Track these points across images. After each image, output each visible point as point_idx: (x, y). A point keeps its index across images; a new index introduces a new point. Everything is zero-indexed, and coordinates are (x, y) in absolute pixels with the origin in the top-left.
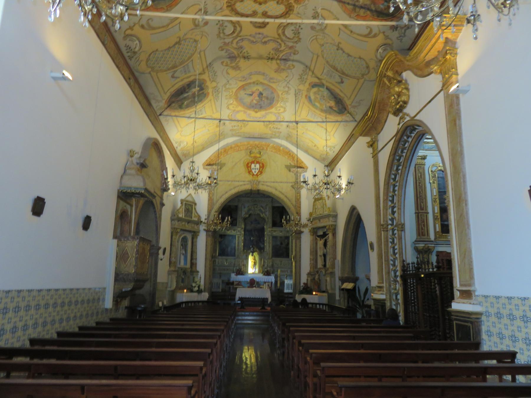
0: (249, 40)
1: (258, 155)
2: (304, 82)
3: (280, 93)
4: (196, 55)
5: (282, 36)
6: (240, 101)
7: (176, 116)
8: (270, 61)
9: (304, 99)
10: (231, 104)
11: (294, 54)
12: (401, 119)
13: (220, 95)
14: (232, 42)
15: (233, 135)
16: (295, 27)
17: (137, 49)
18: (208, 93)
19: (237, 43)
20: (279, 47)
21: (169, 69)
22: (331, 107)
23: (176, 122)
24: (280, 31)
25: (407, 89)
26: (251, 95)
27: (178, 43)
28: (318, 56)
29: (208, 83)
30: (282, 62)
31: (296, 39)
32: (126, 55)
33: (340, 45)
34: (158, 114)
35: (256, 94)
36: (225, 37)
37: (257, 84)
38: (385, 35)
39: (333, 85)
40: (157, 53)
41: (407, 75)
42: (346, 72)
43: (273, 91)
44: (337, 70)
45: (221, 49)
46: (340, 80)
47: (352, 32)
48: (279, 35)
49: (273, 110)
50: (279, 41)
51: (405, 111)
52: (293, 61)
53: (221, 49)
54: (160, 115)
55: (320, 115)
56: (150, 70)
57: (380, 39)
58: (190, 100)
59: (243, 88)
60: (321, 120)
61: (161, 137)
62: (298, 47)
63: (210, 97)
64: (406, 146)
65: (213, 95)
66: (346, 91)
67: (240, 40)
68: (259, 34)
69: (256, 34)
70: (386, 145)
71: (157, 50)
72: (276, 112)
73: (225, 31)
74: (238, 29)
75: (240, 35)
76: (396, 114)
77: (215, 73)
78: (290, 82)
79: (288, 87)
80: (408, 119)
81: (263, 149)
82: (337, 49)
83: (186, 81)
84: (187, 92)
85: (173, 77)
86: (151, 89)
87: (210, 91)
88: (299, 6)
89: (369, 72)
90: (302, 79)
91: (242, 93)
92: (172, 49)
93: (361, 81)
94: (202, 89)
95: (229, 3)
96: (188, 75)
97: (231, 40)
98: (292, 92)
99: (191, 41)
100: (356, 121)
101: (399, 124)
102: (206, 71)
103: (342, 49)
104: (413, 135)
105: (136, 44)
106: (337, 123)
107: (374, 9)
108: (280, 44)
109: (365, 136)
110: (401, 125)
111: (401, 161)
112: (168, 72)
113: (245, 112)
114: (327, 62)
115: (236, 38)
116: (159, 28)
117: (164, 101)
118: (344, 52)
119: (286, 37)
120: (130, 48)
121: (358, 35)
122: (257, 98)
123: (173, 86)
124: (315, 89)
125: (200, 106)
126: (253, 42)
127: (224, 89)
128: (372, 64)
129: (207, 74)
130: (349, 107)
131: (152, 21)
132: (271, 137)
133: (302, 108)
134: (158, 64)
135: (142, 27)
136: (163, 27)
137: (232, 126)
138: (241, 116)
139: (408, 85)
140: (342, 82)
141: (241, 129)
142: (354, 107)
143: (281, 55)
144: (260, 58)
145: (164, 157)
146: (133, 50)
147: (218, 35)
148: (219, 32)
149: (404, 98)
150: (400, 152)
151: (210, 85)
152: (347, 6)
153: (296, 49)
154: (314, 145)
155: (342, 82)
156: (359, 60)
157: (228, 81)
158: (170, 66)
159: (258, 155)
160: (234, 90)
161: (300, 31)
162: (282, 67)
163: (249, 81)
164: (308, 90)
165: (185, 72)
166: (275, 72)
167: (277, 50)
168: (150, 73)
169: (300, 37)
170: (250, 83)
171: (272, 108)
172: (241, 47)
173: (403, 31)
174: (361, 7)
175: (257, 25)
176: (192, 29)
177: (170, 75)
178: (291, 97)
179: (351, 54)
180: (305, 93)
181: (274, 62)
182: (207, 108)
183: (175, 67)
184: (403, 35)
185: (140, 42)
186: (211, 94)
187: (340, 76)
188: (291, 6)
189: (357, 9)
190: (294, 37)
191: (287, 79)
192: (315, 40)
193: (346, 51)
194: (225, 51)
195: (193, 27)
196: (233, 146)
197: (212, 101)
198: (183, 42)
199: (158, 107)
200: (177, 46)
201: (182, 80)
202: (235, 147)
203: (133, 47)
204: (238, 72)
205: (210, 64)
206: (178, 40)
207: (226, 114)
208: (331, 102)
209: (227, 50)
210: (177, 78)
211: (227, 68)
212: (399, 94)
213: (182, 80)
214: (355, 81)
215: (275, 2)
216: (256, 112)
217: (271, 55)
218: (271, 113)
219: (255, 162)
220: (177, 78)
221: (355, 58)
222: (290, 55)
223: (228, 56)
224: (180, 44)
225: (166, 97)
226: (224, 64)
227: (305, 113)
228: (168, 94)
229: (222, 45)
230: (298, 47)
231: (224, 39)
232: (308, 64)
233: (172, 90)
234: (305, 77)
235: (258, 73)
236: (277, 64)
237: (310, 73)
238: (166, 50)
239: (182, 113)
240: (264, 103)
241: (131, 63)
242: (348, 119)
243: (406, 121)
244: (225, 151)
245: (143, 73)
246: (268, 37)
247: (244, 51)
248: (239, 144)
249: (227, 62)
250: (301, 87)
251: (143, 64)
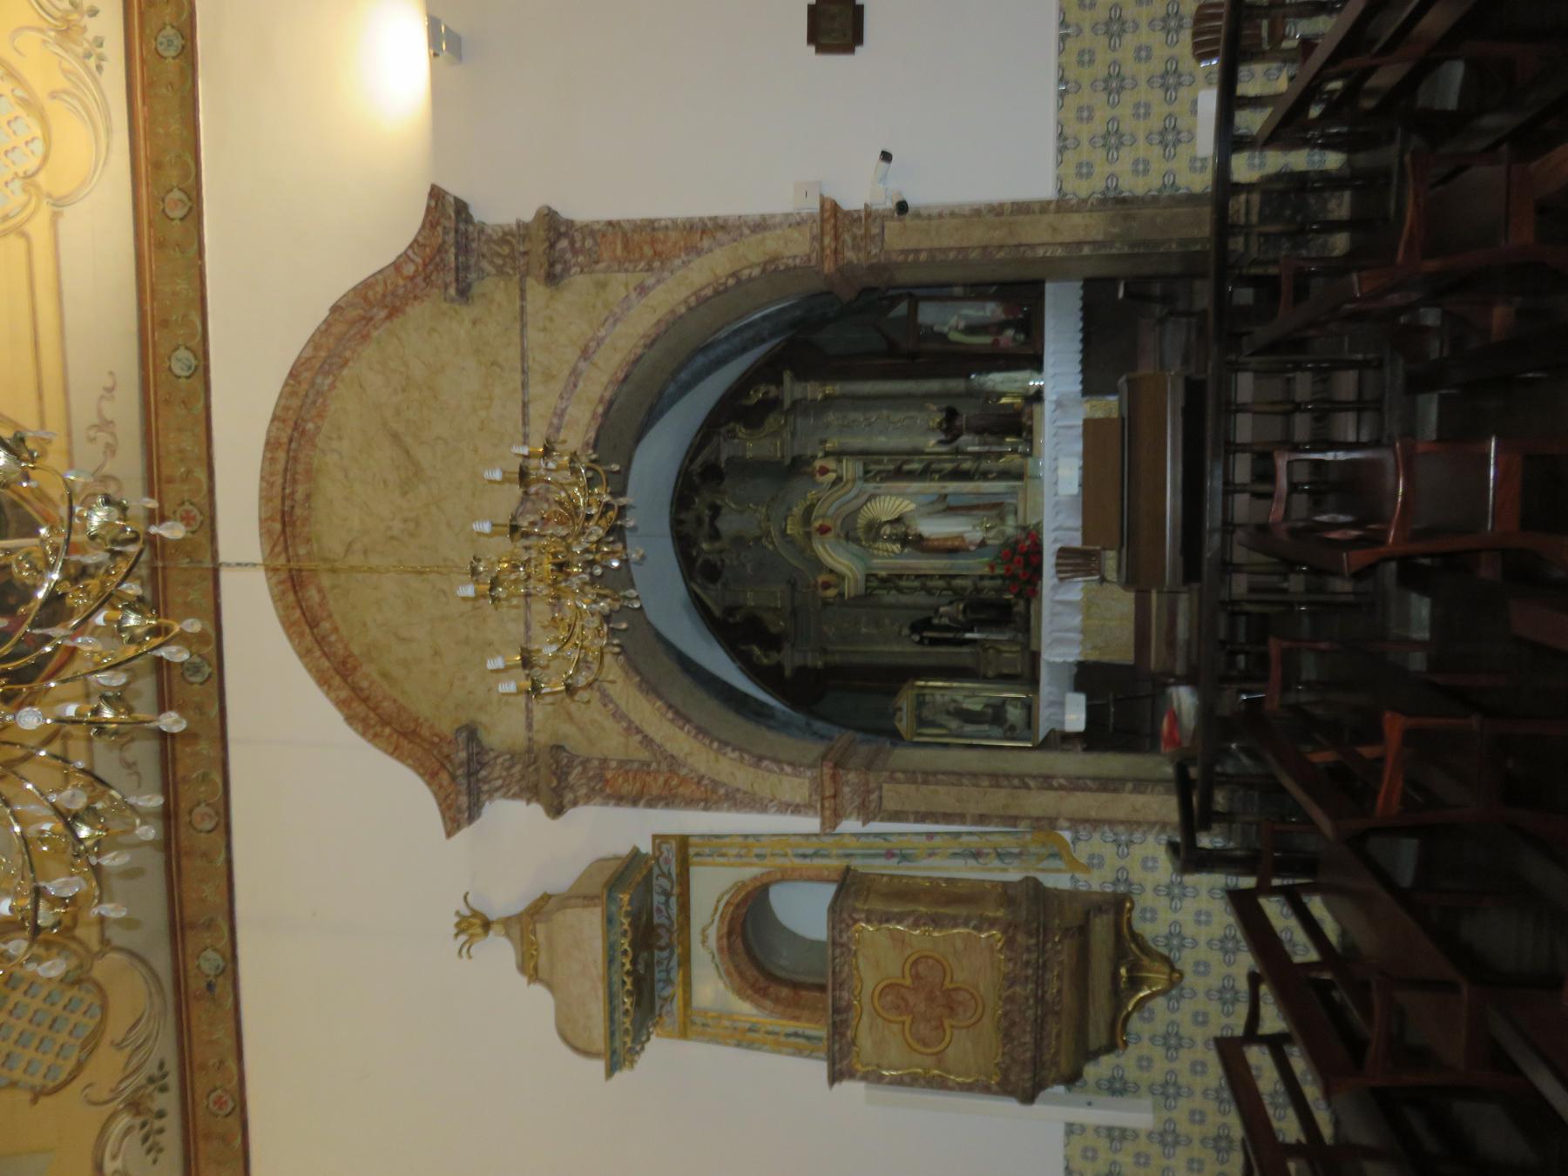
17: (124, 1120)
32: (168, 1101)
40: (37, 1081)
71: (34, 1101)
105: (114, 1157)
120: (145, 1139)
146: (138, 1121)
203: (137, 1135)
251: (116, 1028)
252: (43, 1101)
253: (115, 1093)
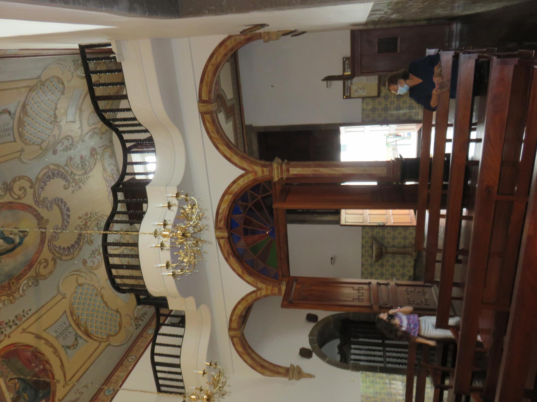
39: (56, 351)
44: (78, 325)
93: (103, 345)
156: (115, 313)
214: (97, 344)
221: (112, 310)
234: (9, 330)
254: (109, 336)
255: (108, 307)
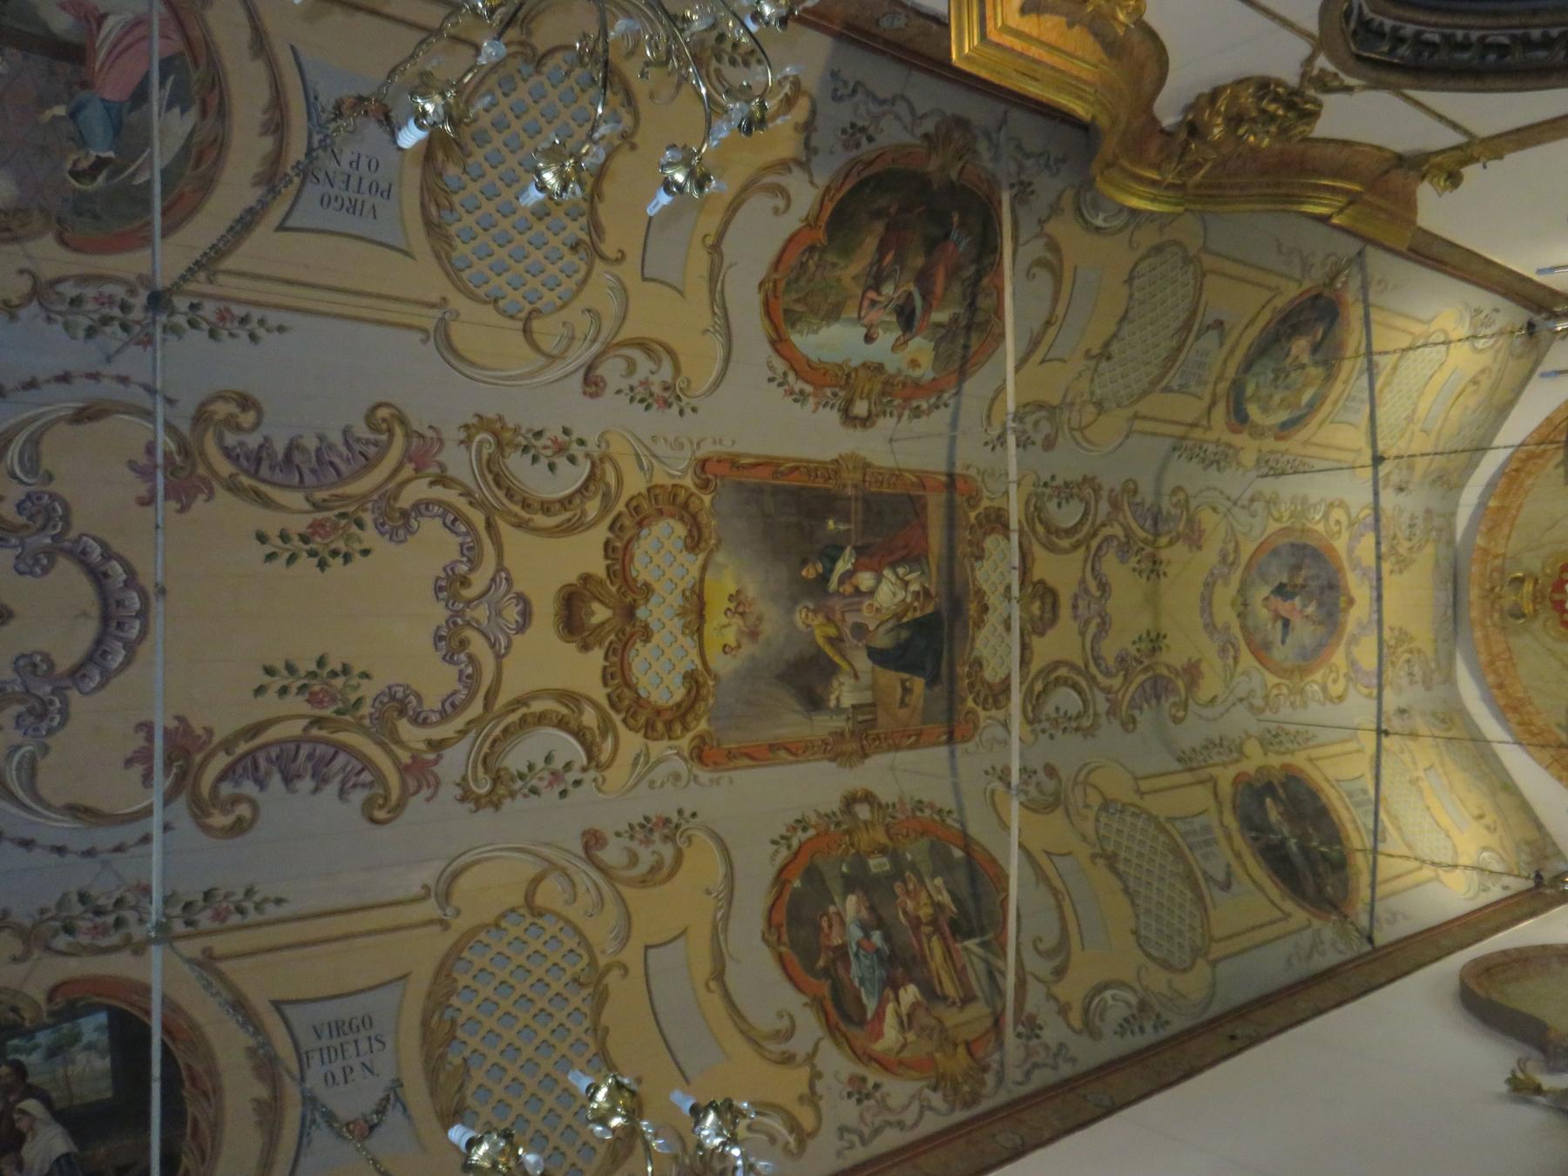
0: (1096, 638)
1: (1528, 587)
2: (1231, 452)
3: (1277, 526)
4: (1150, 803)
5: (1079, 536)
6: (1311, 658)
7: (1373, 886)
8: (1162, 568)
9: (1294, 445)
10: (1324, 689)
11: (1135, 492)
12: (1327, 89)
13: (1292, 728)
14: (1107, 690)
15: (1450, 679)
16: (1050, 498)
17: (1133, 1000)
18: (1285, 767)
19: (1108, 674)
20: (1115, 543)
21: (1201, 898)
22: (1315, 348)
23: (1396, 885)
24: (1065, 543)
25: (1215, 94)
26: (1286, 623)
27: (1111, 861)
28: (1136, 416)
29: (1249, 767)
30: (1163, 528)
31: (1088, 491)
32: (1150, 1037)
33: (1096, 351)
34: (1367, 948)
35: (1284, 607)
36: (1091, 711)
37: (1245, 604)
38: (1049, 218)
39: (1232, 351)
40: (1143, 932)
41: (1168, 111)
42: (1183, 317)
43: (1268, 550)
44: (1179, 349)
45: (1129, 724)
46: (1213, 335)
47: (1048, 323)
48: (1075, 547)
49: (1340, 545)
50: (1094, 543)
51: (1291, 76)
52: (1158, 493)
53: (1129, 724)
54: (1370, 939)
55: (1346, 382)
56: (1200, 961)
57: (1064, 229)
58: (1310, 830)
59: (1261, 650)
60: (1365, 379)
61: (1462, 947)
62: (1111, 481)
63: (1299, 760)
64: (1436, 38)
65: (1292, 752)
66: (1246, 307)
67: (1098, 665)
68: (1075, 607)
69: (1075, 617)
70: (1441, 118)
72: (1345, 535)
73: (1073, 712)
74: (1063, 672)
75: (1080, 664)
76: (1313, 116)
77: (1210, 745)
78: (1233, 497)
79: (1252, 500)
80: (1322, 62)
81: (1502, 571)
82: (1109, 358)
83: (1239, 842)
84: (1283, 841)
85: (1226, 886)
86: (1271, 968)
87: (1275, 761)
88: (986, 493)
89: (1175, 243)
90: (1221, 459)
91: (1278, 653)
92: (1131, 884)
93: (1208, 261)
94: (1269, 788)
95: (985, 700)
96: (1218, 833)
97: (1100, 698)
98: (1268, 486)
99: (1103, 819)
100: (1360, 253)
101: (1348, 89)
102: (1204, 774)
103: (1107, 344)
104: (1389, 23)
106: (1375, 315)
107: (973, 268)
108: (1107, 539)
109: (1410, 204)
110: (1350, 81)
111: (1504, 40)
112: (1208, 900)
113: (1354, 640)
114: (1154, 383)
115: (1094, 678)
116: (1062, 919)
117: (1316, 923)
118: (1114, 336)
119: (1081, 522)
120: (1126, 1020)
121: (1055, 301)
122: (1297, 601)
123: (1261, 888)
124: (1253, 411)
125: (1335, 799)
126: (1104, 626)
127: (1268, 714)
128: (1148, 237)
129: (1216, 771)
130: (1307, 284)
131: (1041, 940)
132: (1450, 542)
133: (1327, 447)
134: (1180, 933)
135: (1060, 972)
136: (1060, 907)
137: (1412, 683)
138: (1367, 655)
139: (1199, 97)
140: (1219, 324)
141: (1419, 651)
142: (1306, 267)
143: (1142, 534)
144: (1152, 601)
145: (1544, 947)
146: (1135, 1011)
147: (1089, 733)
148: (1077, 729)
149: (1247, 99)
150: (1466, 56)
151: (1255, 760)
152: (973, 349)
153: (1118, 488)
154: (1472, 388)
155: (1219, 324)
156: (1136, 282)
157: (1241, 700)
158: (1189, 895)
159: (1528, 587)
160: (1272, 679)
161: (1059, 481)
162: (1181, 527)
163: (1236, 631)
164: (1258, 432)
165: (1207, 843)
166: (1200, 548)
167: (1126, 548)
168: (1214, 964)
169: (1080, 479)
170: (1244, 628)
171: (1332, 549)
172: (1122, 660)
173: (1029, 163)
174: (972, 307)
175: (1048, 615)
176: (1068, 815)
177: (1217, 892)
178: (1288, 488)
179: (1120, 312)
180: (1269, 443)
181: (1164, 554)
182: (1339, 772)
183: (1190, 878)
184: (1042, 161)
185: (1107, 986)
186: (1287, 759)
187: (1198, 337)
188: (987, 516)
189: (980, 317)
190: (1081, 500)
191: (1221, 509)
192: (1087, 432)
193: (1113, 328)
194: (1136, 713)
195: (1060, 812)
196: (1491, 679)
197: (1314, 753)
198: (1110, 848)
199: (1341, 946)
200: (1121, 866)
201: (1238, 855)
202: (1495, 672)
203: (1126, 1012)
204: (1204, 667)
205: (1179, 760)
206: (1101, 862)
207: (1359, 709)
208: (1294, 351)
209: (1133, 704)
210: (1229, 874)
211: (1192, 707)
212: (1236, 120)
213: (1238, 855)
214: (1210, 280)
215: (977, 565)
216: (1351, 602)
217: (1143, 566)
218: (1350, 550)
219: (1557, 597)
220: (1229, 874)
221: (1131, 296)
222: (1142, 504)
223: (1154, 702)
224: (1115, 855)
225: (1300, 915)
226: (1181, 714)
227: (1342, 433)
228: (1289, 906)
229: (1116, 723)
230: (1111, 481)
231: (1096, 714)
232: (1169, 442)
233: (1274, 892)
234: (1211, 448)
235: (1207, 602)
236: (1171, 543)
237: (1197, 433)
238: (1133, 903)
239: (1361, 862)
240: (1317, 577)
241: (1178, 1024)
242: (1355, 284)
243: (1331, 68)
244: (1510, 708)
245: (1213, 985)
246: (1083, 581)
247: (1133, 650)
248: (1483, 658)
249: (1174, 704)
250: (1248, 458)
252: (1132, 938)
253: (1146, 989)
254: (1187, 260)
255: (1127, 311)
